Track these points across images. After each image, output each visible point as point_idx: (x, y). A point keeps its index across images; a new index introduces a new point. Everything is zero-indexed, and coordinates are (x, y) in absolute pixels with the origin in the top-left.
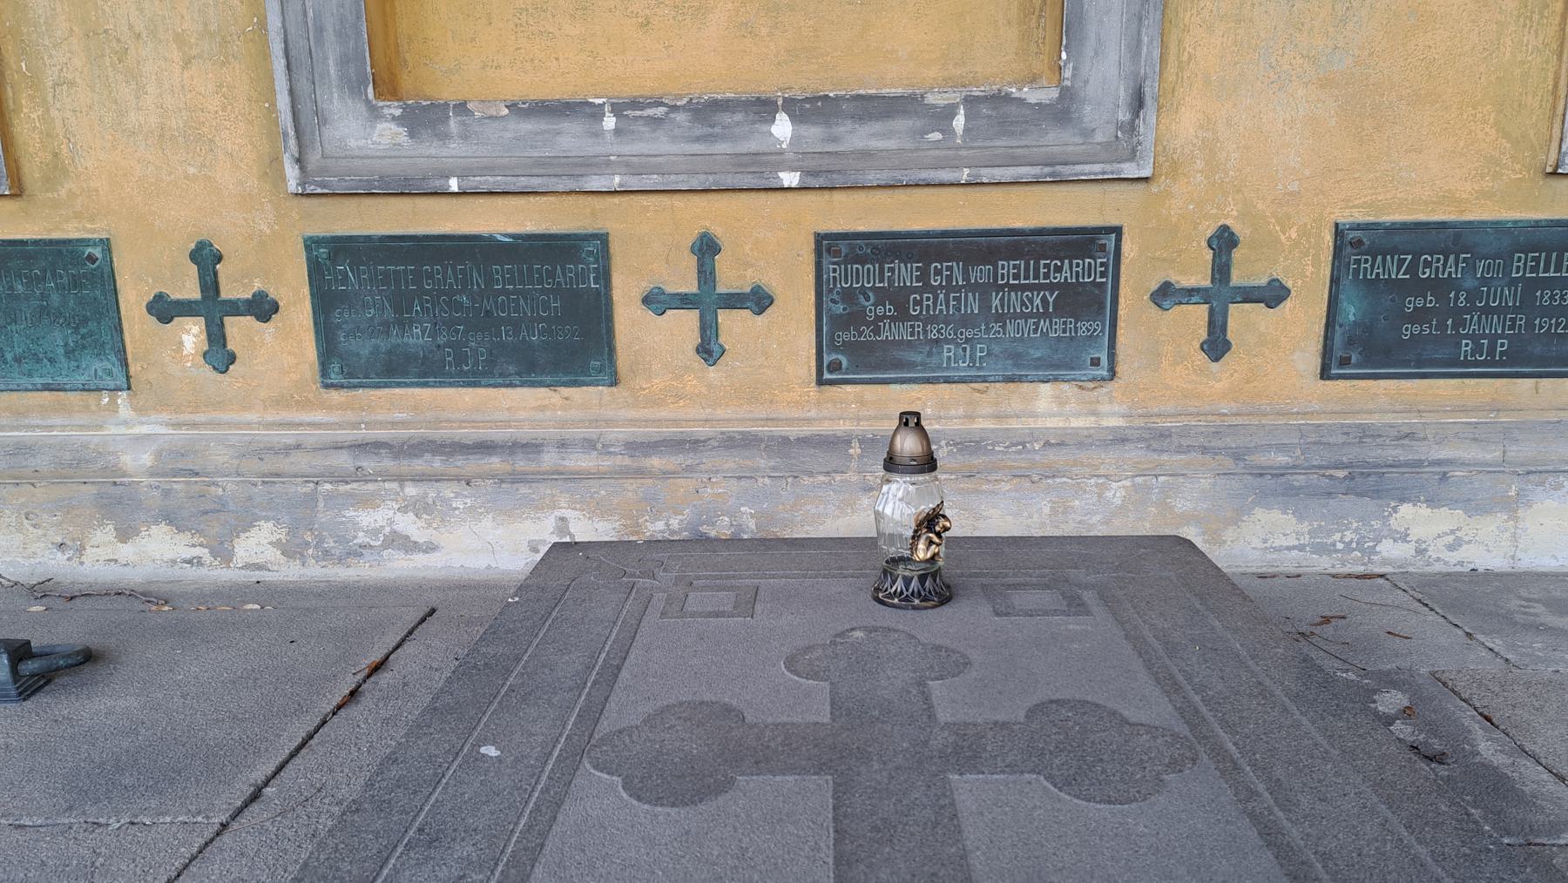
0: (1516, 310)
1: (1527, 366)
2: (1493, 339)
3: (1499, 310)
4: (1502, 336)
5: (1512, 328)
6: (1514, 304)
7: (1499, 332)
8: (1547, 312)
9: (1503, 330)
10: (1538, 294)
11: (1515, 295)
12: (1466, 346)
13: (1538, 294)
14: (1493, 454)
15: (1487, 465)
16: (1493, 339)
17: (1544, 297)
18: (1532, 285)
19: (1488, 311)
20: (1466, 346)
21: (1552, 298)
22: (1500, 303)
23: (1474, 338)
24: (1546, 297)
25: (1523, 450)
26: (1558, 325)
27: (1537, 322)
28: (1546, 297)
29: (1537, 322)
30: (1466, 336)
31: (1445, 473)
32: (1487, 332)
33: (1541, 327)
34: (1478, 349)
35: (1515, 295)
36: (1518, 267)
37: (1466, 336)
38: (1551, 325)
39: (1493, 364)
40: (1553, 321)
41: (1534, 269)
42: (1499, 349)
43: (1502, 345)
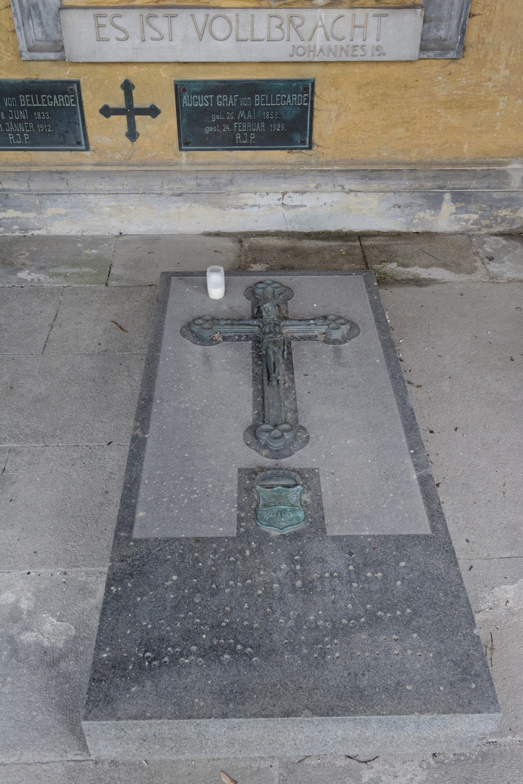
0: (27, 121)
1: (40, 146)
2: (22, 133)
3: (21, 121)
4: (25, 132)
5: (28, 129)
6: (26, 118)
7: (23, 130)
8: (41, 121)
9: (25, 130)
10: (35, 114)
11: (25, 114)
12: (11, 137)
13: (35, 114)
14: (24, 187)
15: (24, 191)
16: (22, 133)
17: (38, 115)
18: (31, 110)
19: (14, 121)
20: (11, 137)
21: (41, 115)
22: (20, 117)
23: (14, 133)
24: (39, 115)
25: (37, 185)
26: (48, 128)
27: (38, 126)
28: (39, 115)
29: (38, 126)
30: (10, 132)
31: (8, 195)
32: (18, 130)
33: (41, 129)
34: (16, 138)
35: (25, 114)
36: (23, 102)
37: (10, 132)
38: (45, 128)
39: (25, 145)
40: (45, 126)
41: (30, 102)
42: (26, 138)
43: (27, 136)
